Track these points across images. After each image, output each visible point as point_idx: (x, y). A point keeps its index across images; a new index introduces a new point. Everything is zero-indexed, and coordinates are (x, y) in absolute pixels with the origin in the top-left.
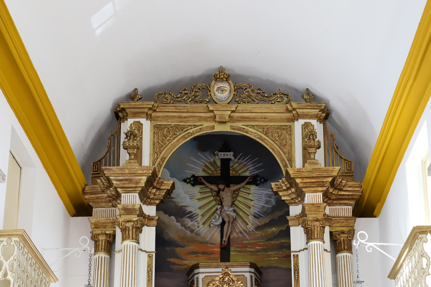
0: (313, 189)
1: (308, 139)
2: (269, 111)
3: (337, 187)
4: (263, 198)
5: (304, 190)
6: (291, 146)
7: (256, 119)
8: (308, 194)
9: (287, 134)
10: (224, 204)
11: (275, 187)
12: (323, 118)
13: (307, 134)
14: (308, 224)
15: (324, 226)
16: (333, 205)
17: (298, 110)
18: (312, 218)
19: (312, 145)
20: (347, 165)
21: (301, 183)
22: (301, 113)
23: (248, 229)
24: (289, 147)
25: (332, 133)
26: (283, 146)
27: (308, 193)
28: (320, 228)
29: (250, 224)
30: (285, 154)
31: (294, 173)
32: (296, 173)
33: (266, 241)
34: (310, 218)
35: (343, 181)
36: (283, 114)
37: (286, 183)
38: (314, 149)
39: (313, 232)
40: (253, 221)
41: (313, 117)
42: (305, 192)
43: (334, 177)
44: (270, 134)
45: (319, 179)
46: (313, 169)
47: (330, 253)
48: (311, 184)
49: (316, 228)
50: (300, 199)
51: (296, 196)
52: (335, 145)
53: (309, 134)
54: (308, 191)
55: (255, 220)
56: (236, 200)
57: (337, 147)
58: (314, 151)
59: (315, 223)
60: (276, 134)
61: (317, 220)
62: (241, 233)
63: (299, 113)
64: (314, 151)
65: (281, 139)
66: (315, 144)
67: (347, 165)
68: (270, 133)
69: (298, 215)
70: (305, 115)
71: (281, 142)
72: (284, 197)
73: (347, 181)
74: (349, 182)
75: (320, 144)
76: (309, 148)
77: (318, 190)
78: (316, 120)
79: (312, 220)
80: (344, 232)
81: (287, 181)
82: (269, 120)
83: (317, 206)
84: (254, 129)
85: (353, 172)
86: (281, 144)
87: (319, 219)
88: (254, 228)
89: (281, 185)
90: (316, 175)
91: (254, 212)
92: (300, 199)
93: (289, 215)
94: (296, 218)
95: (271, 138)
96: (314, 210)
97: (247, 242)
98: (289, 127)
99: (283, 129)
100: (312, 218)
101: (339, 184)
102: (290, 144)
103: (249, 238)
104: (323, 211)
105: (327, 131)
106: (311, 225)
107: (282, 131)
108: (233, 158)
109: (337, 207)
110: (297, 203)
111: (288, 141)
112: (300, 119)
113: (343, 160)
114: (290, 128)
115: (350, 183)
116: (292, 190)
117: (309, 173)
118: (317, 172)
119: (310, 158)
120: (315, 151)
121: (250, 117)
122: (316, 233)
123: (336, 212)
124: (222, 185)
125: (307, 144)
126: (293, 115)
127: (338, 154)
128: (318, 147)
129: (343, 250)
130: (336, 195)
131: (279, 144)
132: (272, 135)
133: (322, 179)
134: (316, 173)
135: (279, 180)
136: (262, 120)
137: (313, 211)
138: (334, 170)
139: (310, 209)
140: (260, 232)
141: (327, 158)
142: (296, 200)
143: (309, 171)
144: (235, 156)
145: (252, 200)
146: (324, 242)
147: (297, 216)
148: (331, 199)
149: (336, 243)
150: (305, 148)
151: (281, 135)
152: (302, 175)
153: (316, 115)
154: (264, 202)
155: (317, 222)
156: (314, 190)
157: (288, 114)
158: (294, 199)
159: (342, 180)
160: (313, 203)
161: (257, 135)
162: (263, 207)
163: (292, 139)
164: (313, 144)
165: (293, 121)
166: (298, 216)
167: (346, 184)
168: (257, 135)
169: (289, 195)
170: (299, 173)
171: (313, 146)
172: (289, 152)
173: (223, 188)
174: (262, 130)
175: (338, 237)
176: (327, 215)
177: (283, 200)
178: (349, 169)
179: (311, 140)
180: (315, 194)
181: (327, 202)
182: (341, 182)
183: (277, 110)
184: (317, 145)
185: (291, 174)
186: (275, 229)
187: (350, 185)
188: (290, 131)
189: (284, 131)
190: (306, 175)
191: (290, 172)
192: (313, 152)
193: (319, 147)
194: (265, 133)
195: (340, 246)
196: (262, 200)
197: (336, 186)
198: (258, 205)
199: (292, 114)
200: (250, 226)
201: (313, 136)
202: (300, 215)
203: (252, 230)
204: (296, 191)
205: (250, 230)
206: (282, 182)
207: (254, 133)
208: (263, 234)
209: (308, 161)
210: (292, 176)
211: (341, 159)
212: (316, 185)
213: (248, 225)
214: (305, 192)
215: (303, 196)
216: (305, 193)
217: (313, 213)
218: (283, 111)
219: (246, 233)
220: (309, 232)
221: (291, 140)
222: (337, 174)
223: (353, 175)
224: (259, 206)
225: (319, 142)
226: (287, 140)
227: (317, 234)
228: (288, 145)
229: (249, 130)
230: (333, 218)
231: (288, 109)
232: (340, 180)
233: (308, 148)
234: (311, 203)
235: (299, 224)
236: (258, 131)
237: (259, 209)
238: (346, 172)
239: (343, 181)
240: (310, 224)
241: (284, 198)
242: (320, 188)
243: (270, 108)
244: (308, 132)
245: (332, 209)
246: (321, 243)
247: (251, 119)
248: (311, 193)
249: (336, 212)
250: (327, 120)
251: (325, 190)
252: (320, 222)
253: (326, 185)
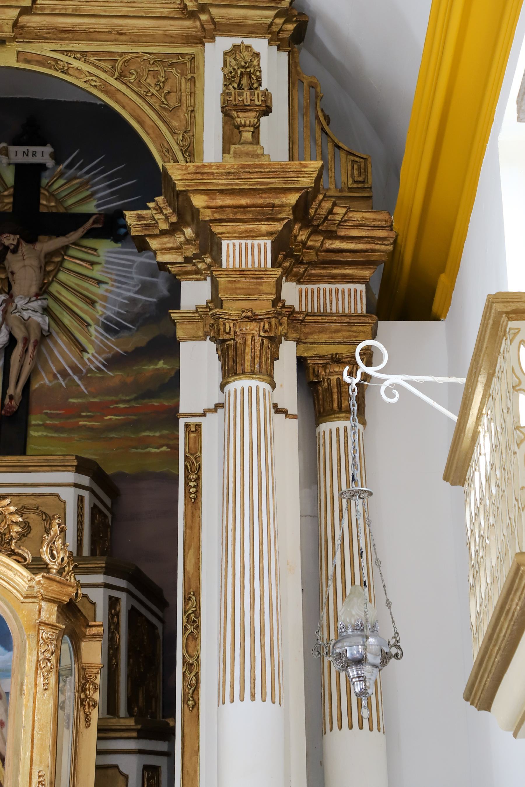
0: (242, 227)
1: (236, 86)
2: (132, 12)
3: (318, 226)
4: (134, 276)
5: (217, 229)
6: (192, 111)
7: (93, 36)
8: (228, 242)
9: (183, 78)
10: (16, 289)
11: (135, 223)
12: (289, 35)
13: (233, 73)
14: (225, 328)
15: (273, 335)
16: (310, 282)
17: (214, 11)
18: (237, 312)
19: (246, 104)
20: (356, 167)
21: (208, 207)
22: (223, 20)
23: (87, 364)
24: (186, 115)
25: (315, 77)
26: (171, 111)
27: (228, 238)
28: (262, 340)
29: (91, 350)
30: (175, 133)
31: (185, 177)
32: (189, 177)
33: (136, 399)
34: (231, 310)
35: (335, 207)
36: (172, 22)
37: (167, 210)
38: (253, 114)
39: (239, 352)
40: (102, 342)
41: (258, 31)
42: (220, 236)
43: (303, 191)
44: (134, 77)
45: (261, 197)
46: (241, 168)
47: (295, 422)
48: (236, 213)
49: (249, 342)
50: (209, 260)
51: (198, 251)
52: (322, 110)
53: (239, 72)
54: (228, 233)
55: (106, 338)
56: (53, 280)
57: (327, 119)
58: (250, 121)
59: (246, 326)
60: (150, 76)
61: (253, 318)
62: (64, 374)
63: (217, 20)
64: (250, 121)
65: (166, 91)
66: (254, 100)
67: (356, 167)
68: (133, 74)
69: (205, 308)
70: (235, 25)
71: (163, 99)
72: (163, 254)
73: (349, 210)
74: (355, 213)
75: (269, 101)
76: (237, 111)
77: (259, 230)
78: (266, 41)
79: (237, 318)
80: (339, 359)
81: (170, 205)
82: (131, 39)
83: (253, 278)
84: (85, 61)
85: (370, 188)
86: (164, 106)
87: (258, 315)
88: (103, 361)
89: (154, 219)
90: (250, 185)
91: (104, 316)
92: (209, 260)
93: (178, 307)
94: (197, 315)
95: (135, 88)
96: (246, 289)
97: (80, 401)
98: (189, 59)
99: (172, 65)
100: (237, 312)
101: (326, 218)
102: (191, 106)
103: (86, 389)
104: (270, 292)
105: (298, 73)
106: (235, 333)
107: (170, 69)
108: (50, 163)
109: (322, 286)
110: (202, 274)
111: (184, 98)
112: (221, 35)
113: (343, 155)
114: (191, 61)
115: (357, 216)
116: (186, 233)
117: (229, 178)
118: (252, 177)
119: (240, 141)
120: (256, 120)
121: (75, 29)
122: (248, 357)
123: (319, 300)
124: (12, 237)
125: (231, 100)
126: (202, 26)
127: (330, 137)
128: (264, 108)
129: (337, 413)
130: (318, 250)
131: (157, 104)
132: (137, 81)
133: (269, 198)
134: (252, 179)
135: (148, 204)
136: (112, 37)
137: (242, 291)
138: (304, 171)
139: (233, 286)
140: (120, 374)
141: (296, 147)
142: (198, 262)
143: (229, 173)
144: (58, 158)
145: (100, 282)
146: (273, 386)
147: (201, 310)
148: (302, 263)
149: (317, 392)
150: (226, 111)
151: (167, 80)
152: (208, 184)
153: (266, 26)
154: (134, 286)
155: (252, 323)
156: (246, 231)
157: (188, 23)
158: (194, 261)
159: (334, 205)
160: (244, 266)
161: (94, 78)
162: (133, 301)
163: (197, 92)
164: (249, 100)
165: (200, 43)
166: (204, 310)
167: (346, 218)
168: (94, 78)
169: (177, 249)
170: (201, 177)
171: (248, 106)
172: (186, 128)
173: (15, 243)
174: (110, 67)
175: (323, 373)
176: (290, 307)
177: (162, 262)
178: (361, 179)
179: (243, 89)
180: (249, 242)
181: (292, 270)
182: (331, 212)
183: (154, 10)
184: (260, 103)
185: (175, 182)
186: (165, 366)
187: (357, 220)
188: (193, 70)
189: (174, 70)
190: (222, 185)
191: (173, 173)
192: (248, 122)
193: (267, 111)
194: (117, 74)
195: (328, 400)
196: (131, 282)
197: (315, 223)
198: (119, 295)
199: (198, 23)
200: (93, 356)
201: (250, 77)
202: (209, 305)
203: (98, 368)
204: (197, 235)
205: (92, 367)
206: (156, 210)
207: (87, 73)
208: (130, 380)
209: (233, 148)
210: (179, 188)
211: (336, 149)
212: (250, 216)
213: (88, 353)
214: (220, 236)
215: (215, 248)
216: (220, 238)
217: (242, 296)
218: (170, 13)
219: (78, 376)
220: (228, 354)
221: (193, 95)
222: (312, 183)
223: (370, 198)
224: (120, 299)
225: (266, 94)
226: (181, 95)
227: (253, 359)
228: (185, 109)
229: (71, 64)
230: (307, 318)
231: (186, 6)
232: (327, 205)
233: (235, 110)
234: (237, 266)
235: (206, 334)
236: (97, 67)
237: (120, 308)
238: (350, 186)
239: (337, 210)
240: (230, 328)
241: (164, 256)
242: (263, 223)
243: (134, 5)
244: (236, 67)
245: (307, 292)
246: (264, 386)
247: (79, 35)
248: (240, 238)
249: (319, 300)
250: (302, 44)
251: (278, 231)
252: (262, 324)
253: (280, 216)
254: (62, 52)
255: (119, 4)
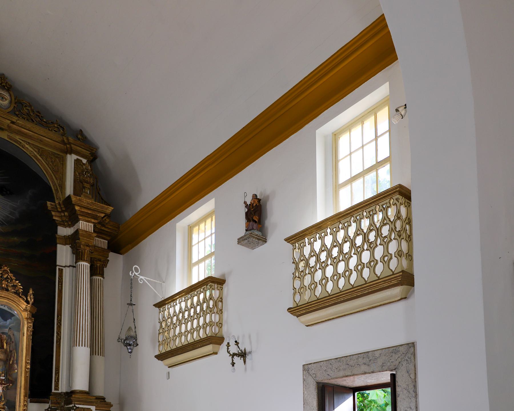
254: (22, 140)
255: (43, 132)
